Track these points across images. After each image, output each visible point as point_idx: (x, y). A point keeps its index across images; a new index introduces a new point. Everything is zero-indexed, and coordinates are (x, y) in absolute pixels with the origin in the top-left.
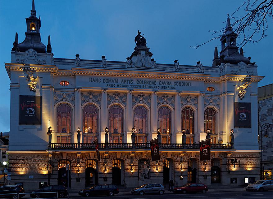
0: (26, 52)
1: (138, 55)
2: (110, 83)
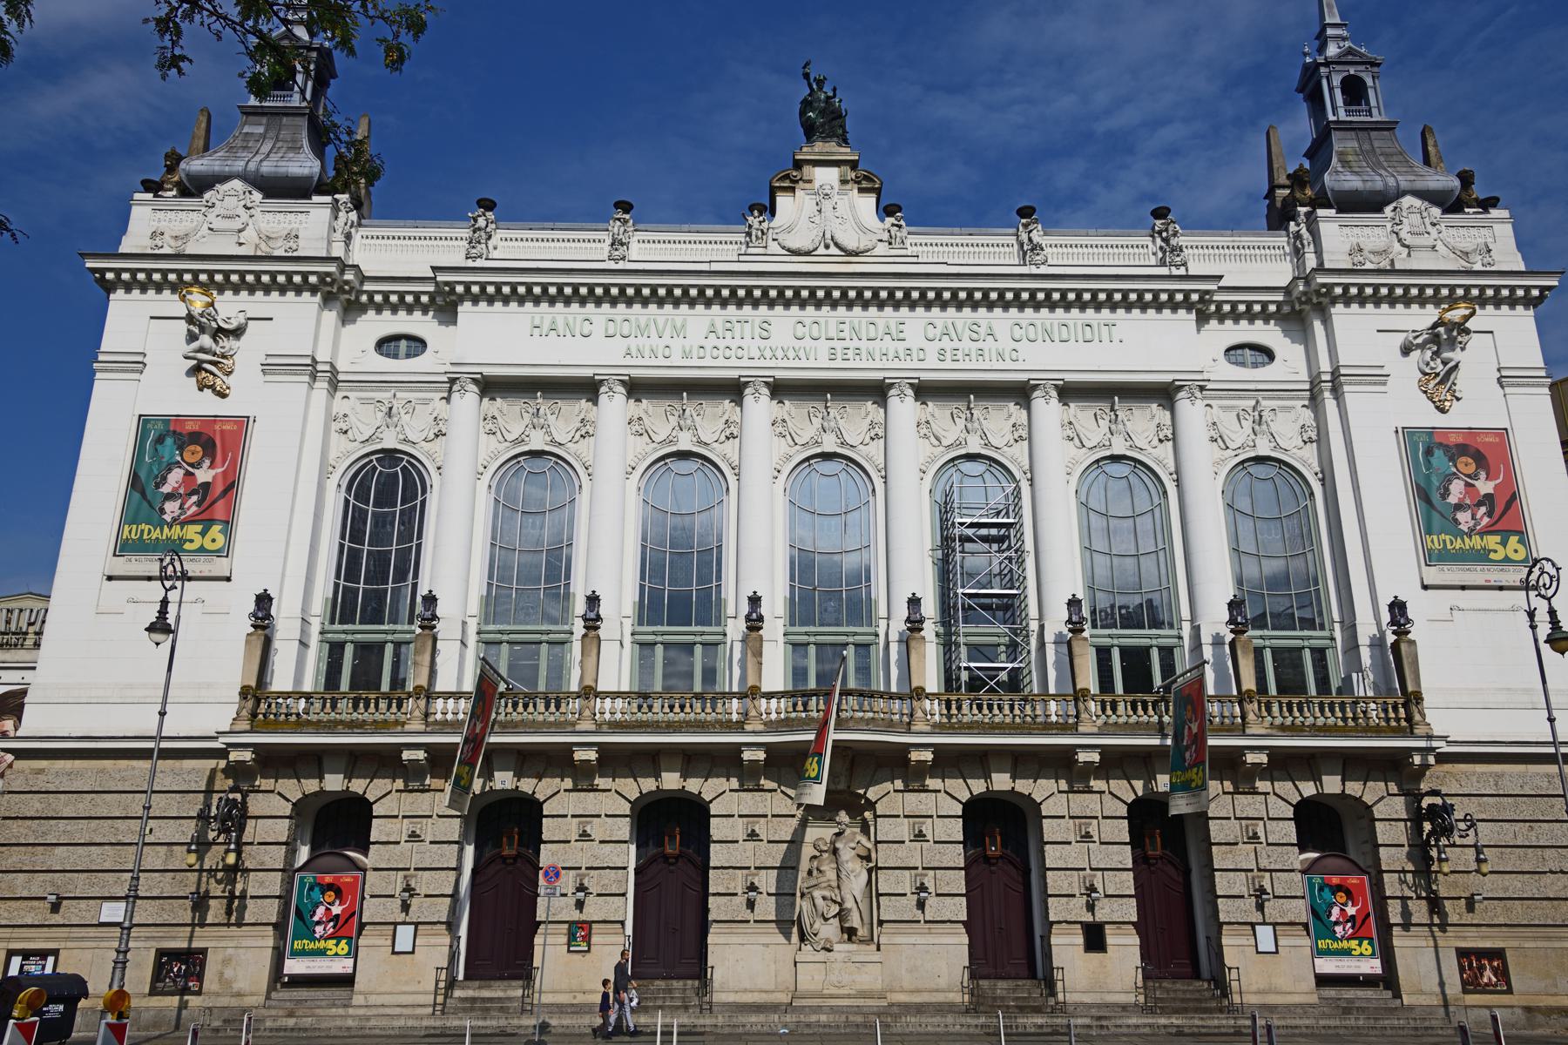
0: (207, 196)
1: (798, 192)
2: (641, 341)
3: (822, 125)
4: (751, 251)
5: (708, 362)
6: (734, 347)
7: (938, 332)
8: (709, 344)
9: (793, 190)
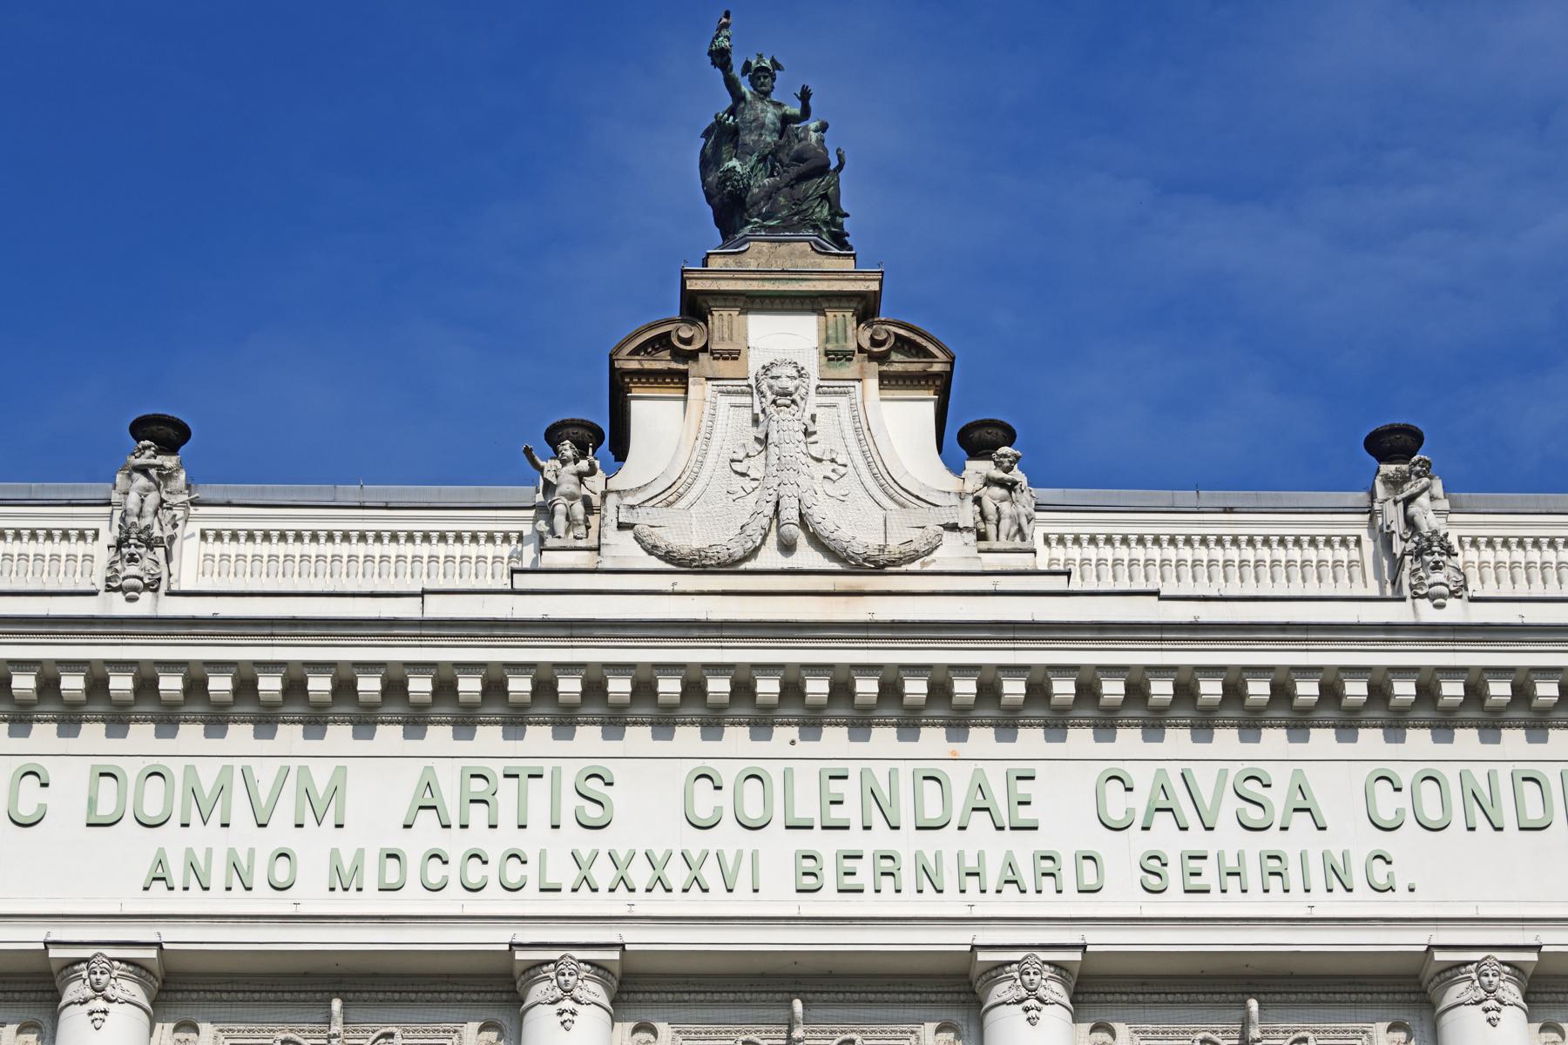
1: (698, 389)
2: (203, 837)
3: (770, 194)
4: (551, 559)
6: (495, 855)
7: (1139, 802)
8: (414, 846)
9: (680, 379)
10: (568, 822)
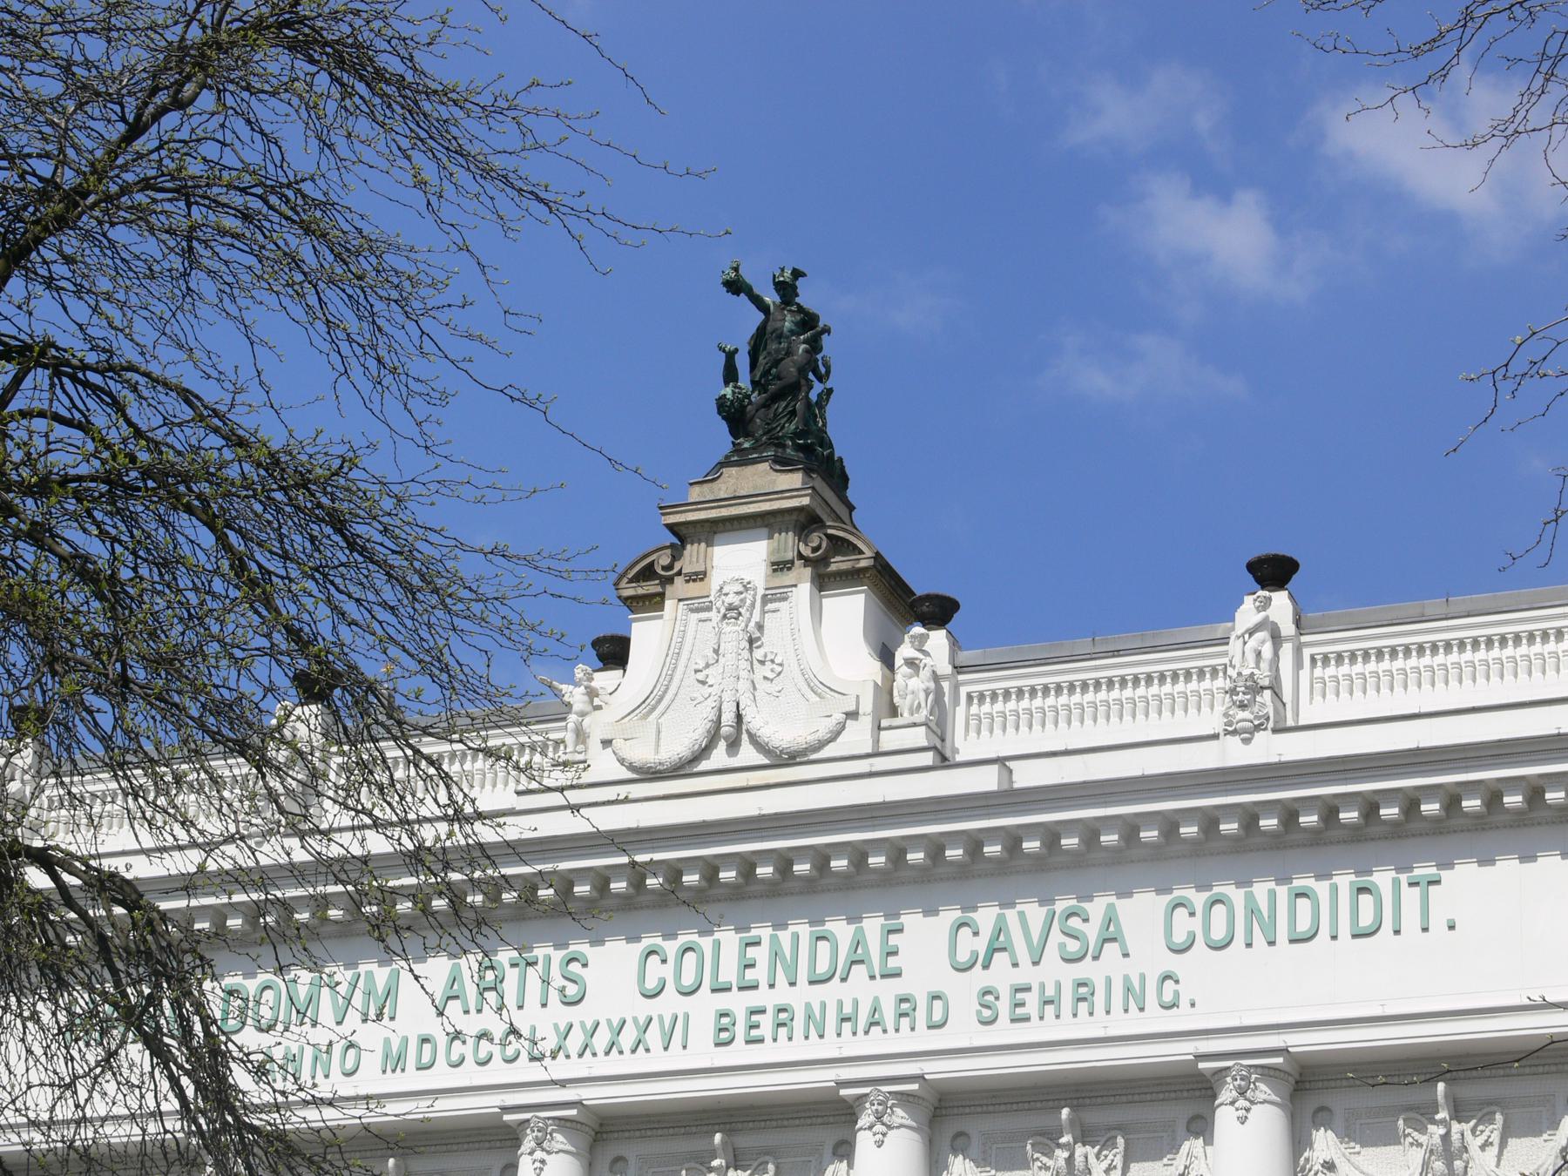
5: (442, 1076)
7: (981, 945)
10: (554, 996)
